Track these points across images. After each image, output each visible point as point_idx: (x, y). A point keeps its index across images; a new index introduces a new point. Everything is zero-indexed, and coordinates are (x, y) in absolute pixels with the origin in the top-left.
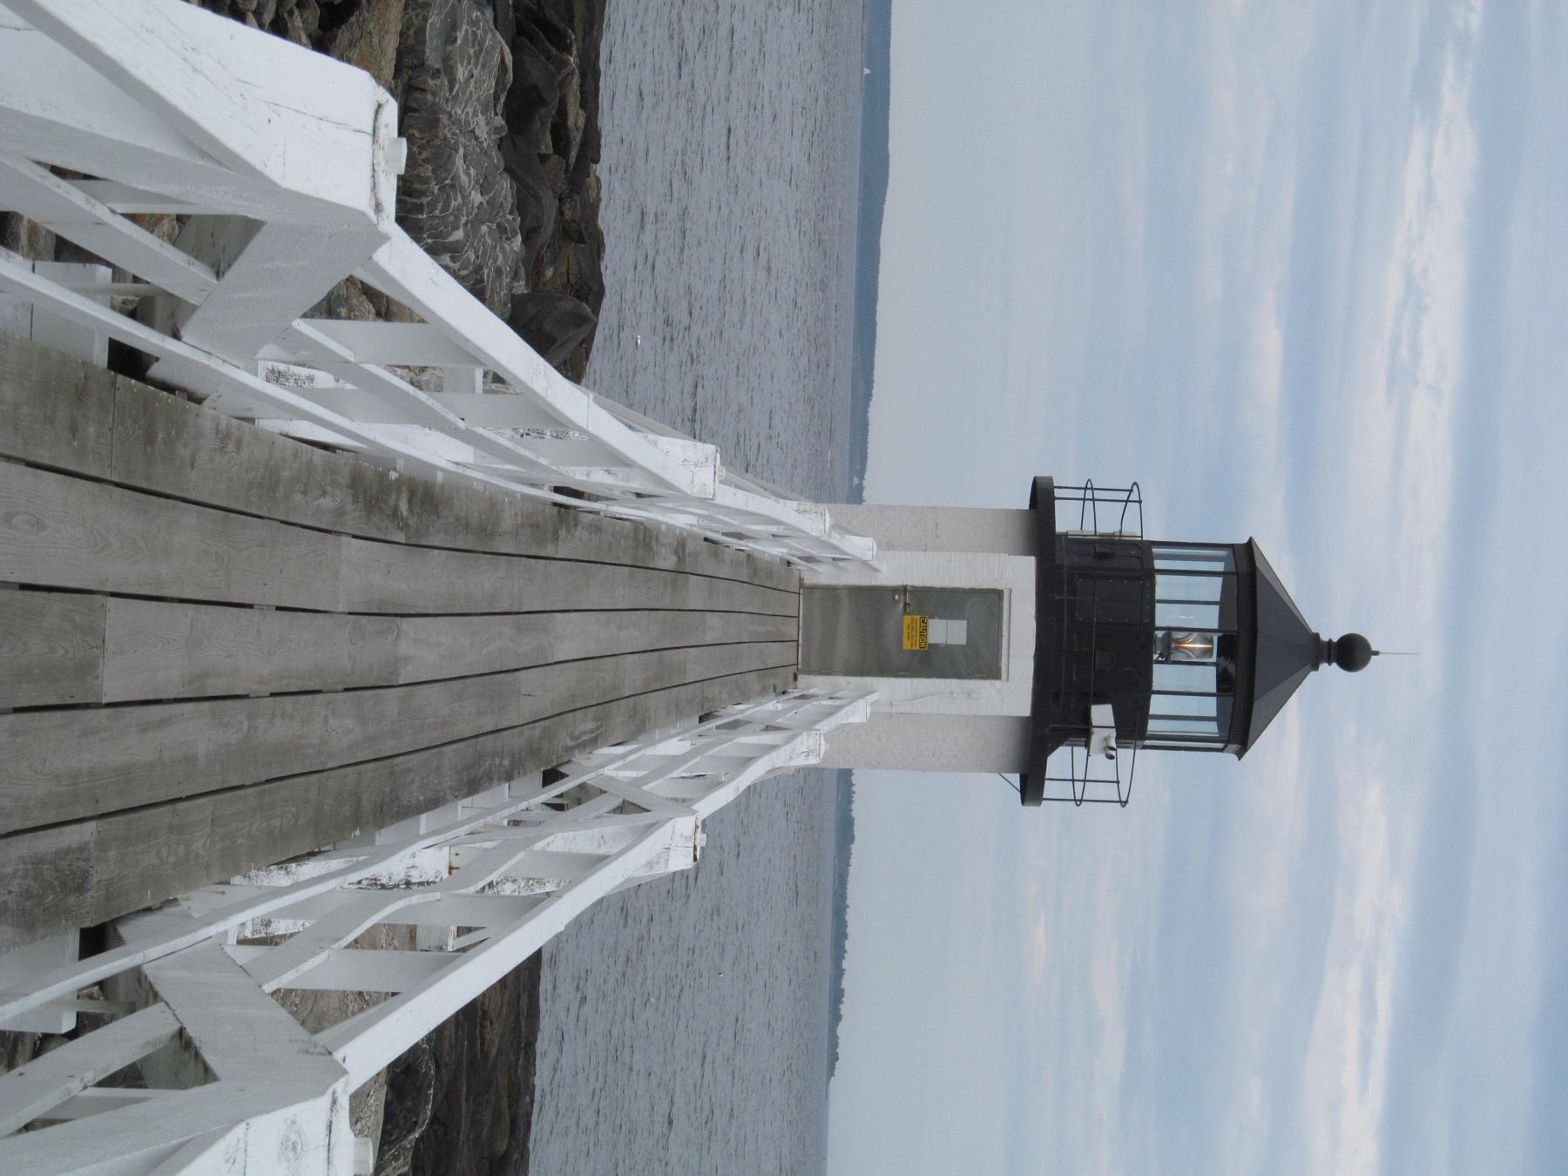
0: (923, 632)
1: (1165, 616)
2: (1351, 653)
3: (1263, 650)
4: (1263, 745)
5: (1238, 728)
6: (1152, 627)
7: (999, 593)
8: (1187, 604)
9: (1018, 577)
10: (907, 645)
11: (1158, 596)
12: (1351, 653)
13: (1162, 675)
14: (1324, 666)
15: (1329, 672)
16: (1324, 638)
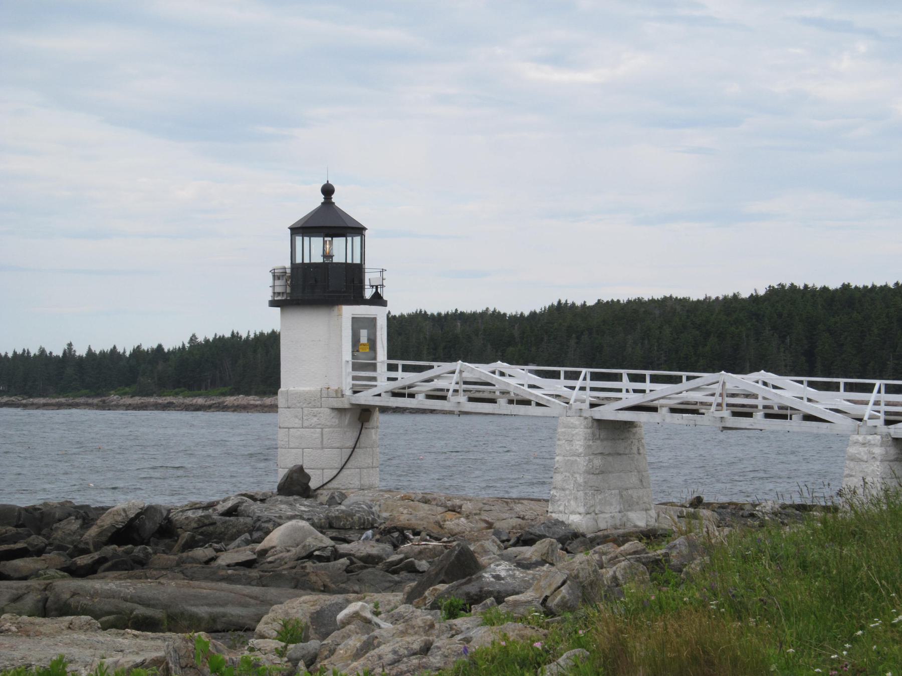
0: (364, 345)
1: (318, 258)
2: (328, 191)
3: (328, 222)
4: (364, 224)
5: (359, 230)
6: (323, 263)
7: (353, 318)
8: (314, 250)
9: (349, 311)
10: (368, 350)
11: (344, 261)
12: (328, 191)
13: (339, 258)
14: (333, 200)
15: (335, 198)
16: (323, 200)
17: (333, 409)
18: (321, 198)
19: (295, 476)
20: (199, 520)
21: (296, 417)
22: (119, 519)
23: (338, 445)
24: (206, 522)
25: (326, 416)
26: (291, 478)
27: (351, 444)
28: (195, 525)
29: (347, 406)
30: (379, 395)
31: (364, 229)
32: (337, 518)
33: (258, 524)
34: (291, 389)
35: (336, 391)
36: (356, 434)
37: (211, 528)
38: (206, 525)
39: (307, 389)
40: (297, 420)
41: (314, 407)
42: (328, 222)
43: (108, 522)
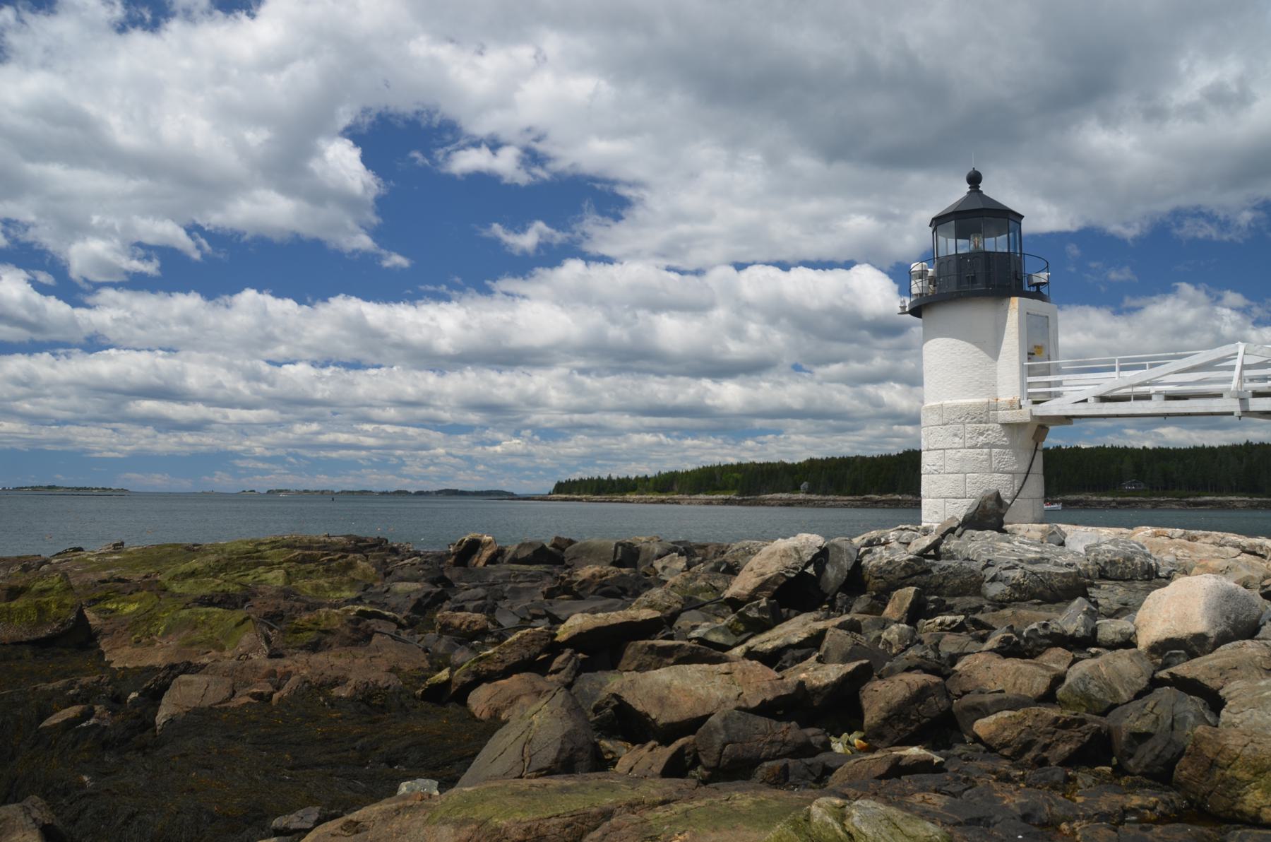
2: (974, 179)
12: (974, 179)
15: (982, 187)
17: (1004, 425)
18: (966, 188)
19: (990, 504)
20: (906, 566)
21: (956, 435)
22: (790, 563)
23: (1009, 469)
24: (918, 568)
25: (995, 433)
26: (984, 507)
27: (1025, 468)
28: (903, 574)
29: (1028, 419)
30: (1086, 401)
31: (1022, 217)
32: (1113, 563)
33: (991, 572)
34: (947, 402)
35: (1011, 403)
36: (1029, 456)
37: (925, 578)
38: (915, 573)
39: (971, 401)
40: (957, 440)
41: (981, 422)
42: (976, 215)
43: (773, 569)
